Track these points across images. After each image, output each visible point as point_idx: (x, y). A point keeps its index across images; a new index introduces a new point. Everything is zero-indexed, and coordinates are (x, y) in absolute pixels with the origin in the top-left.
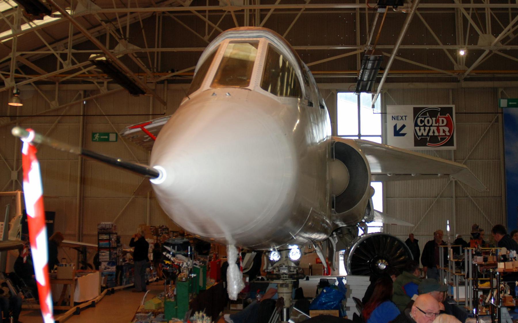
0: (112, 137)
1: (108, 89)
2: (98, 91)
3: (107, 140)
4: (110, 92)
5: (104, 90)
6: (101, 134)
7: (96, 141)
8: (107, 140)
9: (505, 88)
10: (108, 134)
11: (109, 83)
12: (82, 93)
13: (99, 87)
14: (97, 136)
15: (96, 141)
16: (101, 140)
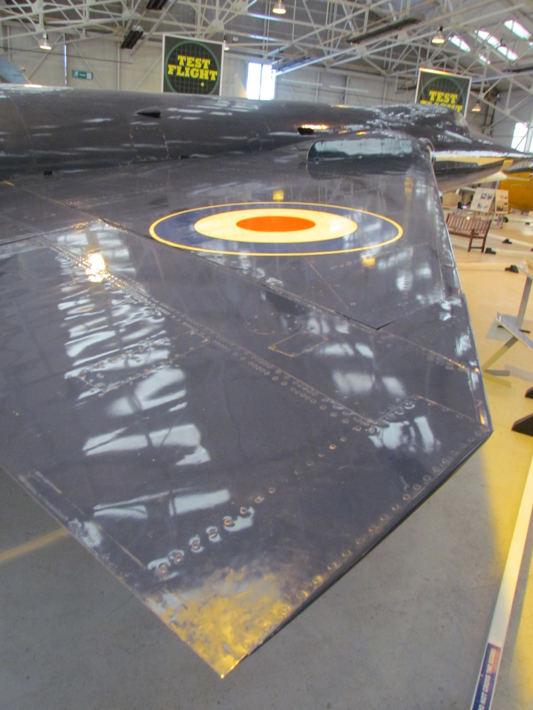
0: (89, 76)
1: (87, 36)
2: (78, 36)
3: (85, 78)
4: (88, 38)
5: (83, 36)
6: (80, 72)
7: (76, 77)
8: (85, 78)
9: (352, 77)
10: (85, 73)
11: (86, 31)
12: (64, 36)
13: (79, 33)
14: (76, 74)
15: (76, 77)
16: (79, 77)
